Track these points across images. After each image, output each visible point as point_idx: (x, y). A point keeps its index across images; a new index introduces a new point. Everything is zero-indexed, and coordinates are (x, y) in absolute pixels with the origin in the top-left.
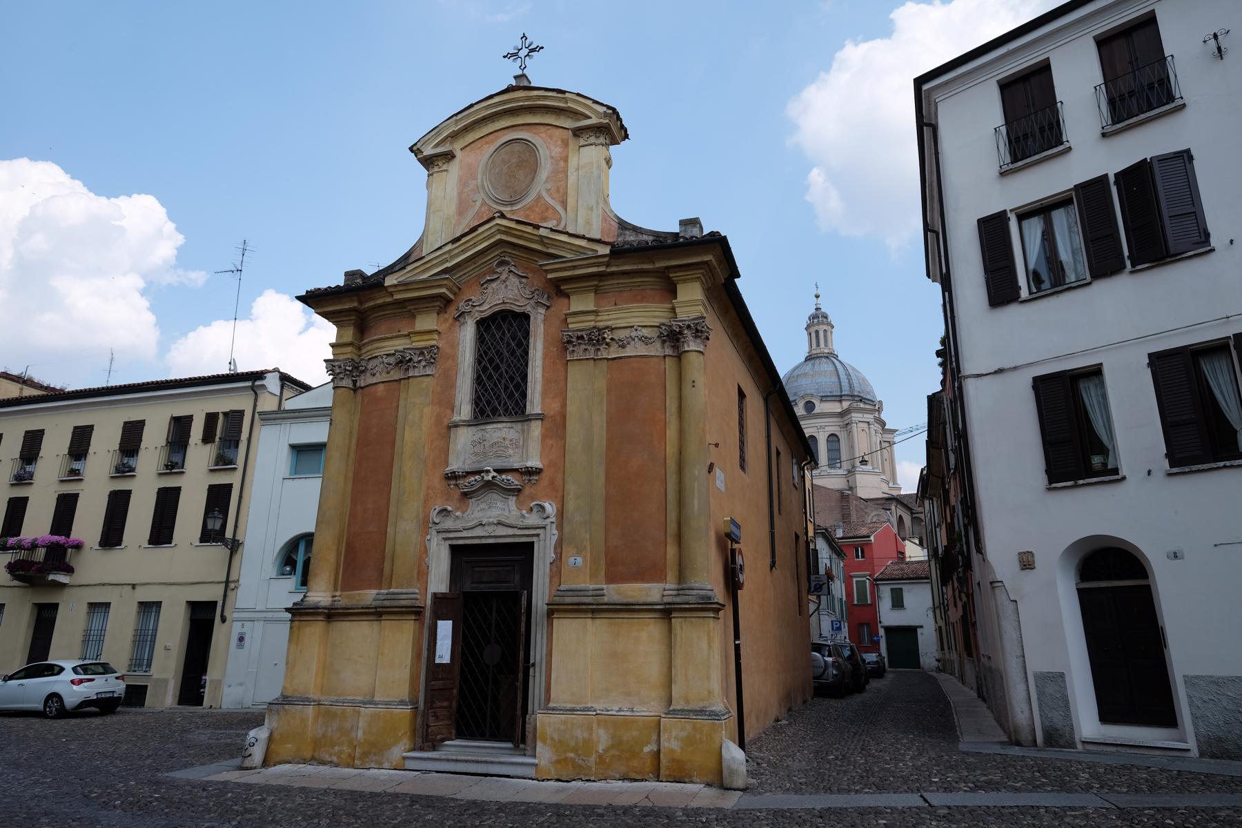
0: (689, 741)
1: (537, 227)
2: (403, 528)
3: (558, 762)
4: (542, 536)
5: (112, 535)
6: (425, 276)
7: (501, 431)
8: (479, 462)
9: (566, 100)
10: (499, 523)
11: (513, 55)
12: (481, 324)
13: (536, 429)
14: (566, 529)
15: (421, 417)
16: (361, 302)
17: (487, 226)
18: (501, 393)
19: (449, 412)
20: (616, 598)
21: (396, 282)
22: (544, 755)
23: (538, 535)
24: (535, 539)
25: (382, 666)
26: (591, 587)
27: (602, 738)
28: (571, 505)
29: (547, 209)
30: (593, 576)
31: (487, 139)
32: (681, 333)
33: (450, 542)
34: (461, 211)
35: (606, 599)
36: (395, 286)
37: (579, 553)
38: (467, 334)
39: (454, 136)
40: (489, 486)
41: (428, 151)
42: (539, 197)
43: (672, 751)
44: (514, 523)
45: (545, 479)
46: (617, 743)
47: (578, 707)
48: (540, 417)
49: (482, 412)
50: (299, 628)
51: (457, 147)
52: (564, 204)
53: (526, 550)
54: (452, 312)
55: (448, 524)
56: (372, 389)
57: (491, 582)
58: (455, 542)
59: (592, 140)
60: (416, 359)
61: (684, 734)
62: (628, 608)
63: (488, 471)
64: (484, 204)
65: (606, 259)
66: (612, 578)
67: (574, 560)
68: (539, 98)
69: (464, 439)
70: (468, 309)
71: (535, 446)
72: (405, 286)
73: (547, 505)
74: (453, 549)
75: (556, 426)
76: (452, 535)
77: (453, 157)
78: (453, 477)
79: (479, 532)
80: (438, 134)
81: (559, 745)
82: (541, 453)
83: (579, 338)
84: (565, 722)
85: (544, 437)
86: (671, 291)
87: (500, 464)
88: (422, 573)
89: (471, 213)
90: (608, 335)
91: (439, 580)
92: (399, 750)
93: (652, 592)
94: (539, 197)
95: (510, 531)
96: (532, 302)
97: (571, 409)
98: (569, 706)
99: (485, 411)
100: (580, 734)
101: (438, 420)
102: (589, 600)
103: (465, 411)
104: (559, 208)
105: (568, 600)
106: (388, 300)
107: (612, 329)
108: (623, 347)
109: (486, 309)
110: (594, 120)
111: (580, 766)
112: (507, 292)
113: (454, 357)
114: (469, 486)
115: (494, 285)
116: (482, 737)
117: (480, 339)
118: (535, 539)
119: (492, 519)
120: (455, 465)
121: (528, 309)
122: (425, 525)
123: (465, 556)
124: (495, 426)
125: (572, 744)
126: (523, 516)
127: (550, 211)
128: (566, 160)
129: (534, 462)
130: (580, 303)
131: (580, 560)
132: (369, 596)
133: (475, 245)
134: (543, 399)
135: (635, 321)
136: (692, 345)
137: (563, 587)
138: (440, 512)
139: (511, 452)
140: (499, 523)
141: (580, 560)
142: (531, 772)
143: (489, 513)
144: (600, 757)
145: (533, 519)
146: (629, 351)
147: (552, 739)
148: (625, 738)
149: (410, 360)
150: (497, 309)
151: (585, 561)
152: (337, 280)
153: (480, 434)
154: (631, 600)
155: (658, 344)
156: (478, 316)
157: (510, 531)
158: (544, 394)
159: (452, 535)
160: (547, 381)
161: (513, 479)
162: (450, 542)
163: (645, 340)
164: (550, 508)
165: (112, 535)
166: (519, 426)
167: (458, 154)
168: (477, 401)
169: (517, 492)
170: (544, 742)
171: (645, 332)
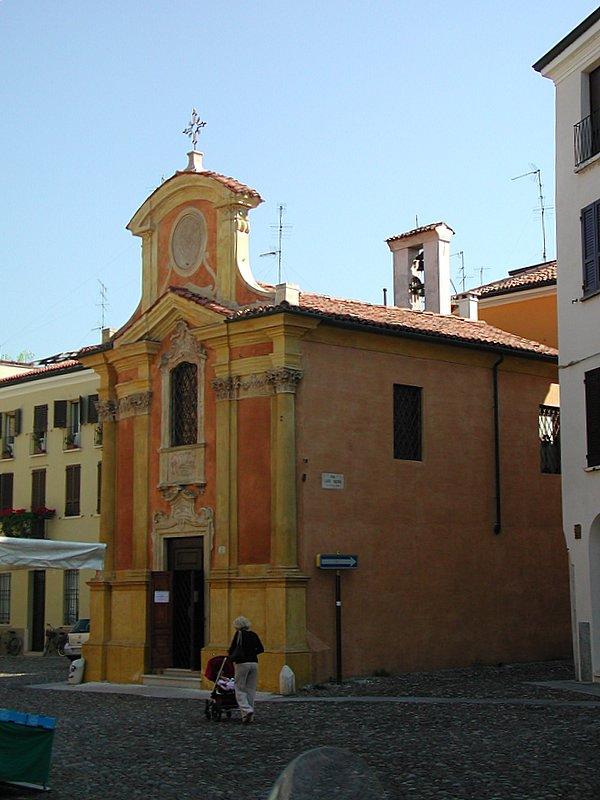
7: (182, 455)
14: (218, 527)
25: (130, 617)
28: (219, 510)
34: (160, 280)
42: (202, 267)
52: (215, 270)
70: (165, 362)
71: (200, 465)
78: (162, 490)
87: (183, 480)
89: (165, 285)
91: (159, 566)
104: (213, 274)
108: (246, 389)
109: (174, 362)
119: (183, 520)
120: (162, 481)
122: (149, 526)
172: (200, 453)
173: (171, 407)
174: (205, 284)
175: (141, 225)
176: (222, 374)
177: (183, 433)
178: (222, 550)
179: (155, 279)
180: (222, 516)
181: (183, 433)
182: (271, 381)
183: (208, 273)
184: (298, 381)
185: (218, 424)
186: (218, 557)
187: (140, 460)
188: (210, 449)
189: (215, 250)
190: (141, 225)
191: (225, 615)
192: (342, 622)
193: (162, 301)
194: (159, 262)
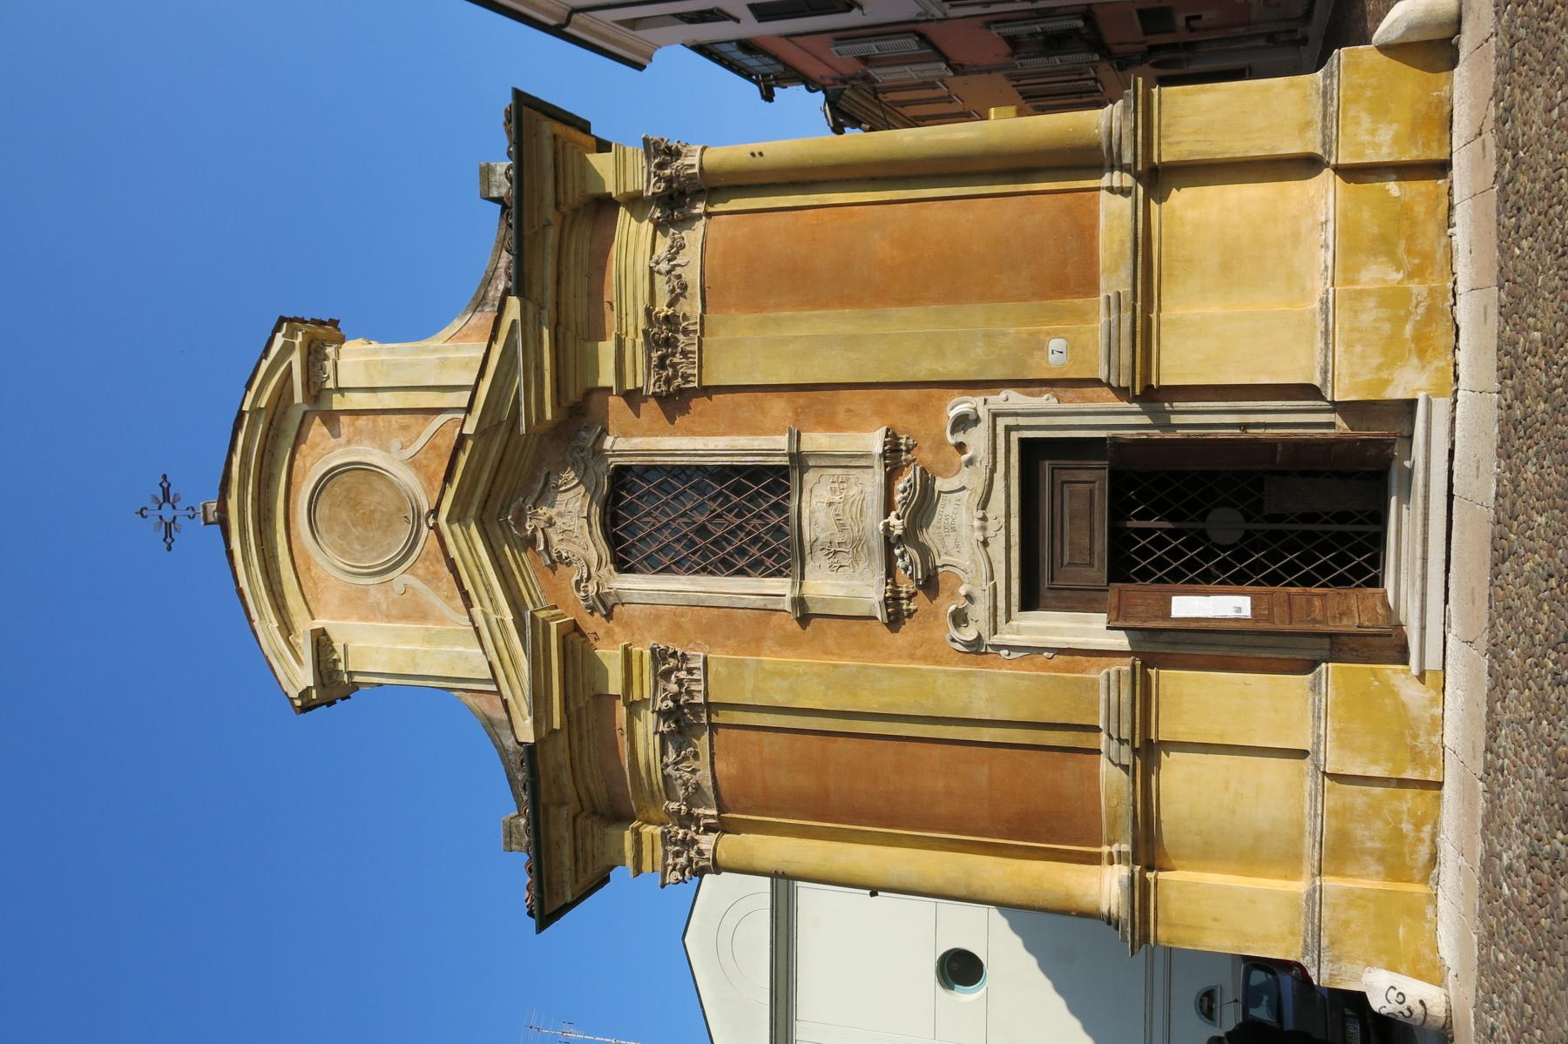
0: (1380, 110)
1: (462, 438)
3: (1421, 354)
4: (1011, 421)
6: (524, 664)
8: (870, 552)
9: (256, 411)
10: (984, 504)
11: (168, 533)
12: (622, 565)
15: (781, 674)
16: (562, 803)
17: (449, 540)
18: (746, 515)
19: (776, 619)
20: (1125, 274)
21: (529, 721)
23: (1008, 429)
24: (1015, 436)
26: (1103, 319)
27: (1377, 274)
29: (434, 447)
30: (1083, 316)
31: (301, 569)
32: (669, 180)
33: (1015, 608)
35: (1126, 289)
36: (536, 722)
37: (1042, 346)
38: (636, 585)
42: (414, 463)
43: (1396, 140)
45: (910, 427)
46: (1384, 247)
47: (1321, 327)
50: (1170, 925)
51: (304, 626)
53: (1033, 452)
54: (593, 624)
55: (979, 612)
56: (723, 784)
57: (1092, 529)
58: (1015, 599)
59: (329, 365)
60: (674, 688)
61: (1366, 121)
63: (887, 526)
65: (530, 306)
66: (1090, 286)
67: (1055, 357)
68: (244, 463)
69: (824, 584)
74: (1030, 602)
75: (815, 396)
76: (1001, 604)
77: (323, 632)
79: (997, 548)
81: (1392, 352)
84: (1349, 345)
85: (831, 425)
90: (662, 308)
91: (1090, 629)
96: (591, 463)
98: (1320, 344)
99: (781, 551)
100: (1370, 315)
101: (788, 642)
102: (1126, 316)
105: (1126, 358)
106: (562, 740)
110: (296, 359)
111: (1429, 309)
115: (555, 538)
116: (1379, 540)
117: (654, 565)
118: (1015, 436)
124: (805, 523)
125: (1387, 328)
126: (970, 462)
127: (439, 441)
129: (875, 442)
131: (1056, 344)
133: (480, 567)
134: (764, 433)
135: (643, 263)
138: (957, 625)
139: (854, 491)
140: (984, 504)
141: (1056, 344)
143: (964, 531)
144: (1410, 276)
145: (977, 440)
146: (692, 276)
147: (1379, 368)
148: (1375, 230)
149: (675, 698)
150: (597, 531)
151: (1056, 334)
153: (820, 554)
154: (1129, 245)
158: (755, 431)
159: (1001, 604)
162: (1015, 608)
163: (677, 249)
164: (962, 404)
167: (319, 623)
168: (755, 568)
170: (1386, 383)
190: (298, 660)
193: (454, 553)
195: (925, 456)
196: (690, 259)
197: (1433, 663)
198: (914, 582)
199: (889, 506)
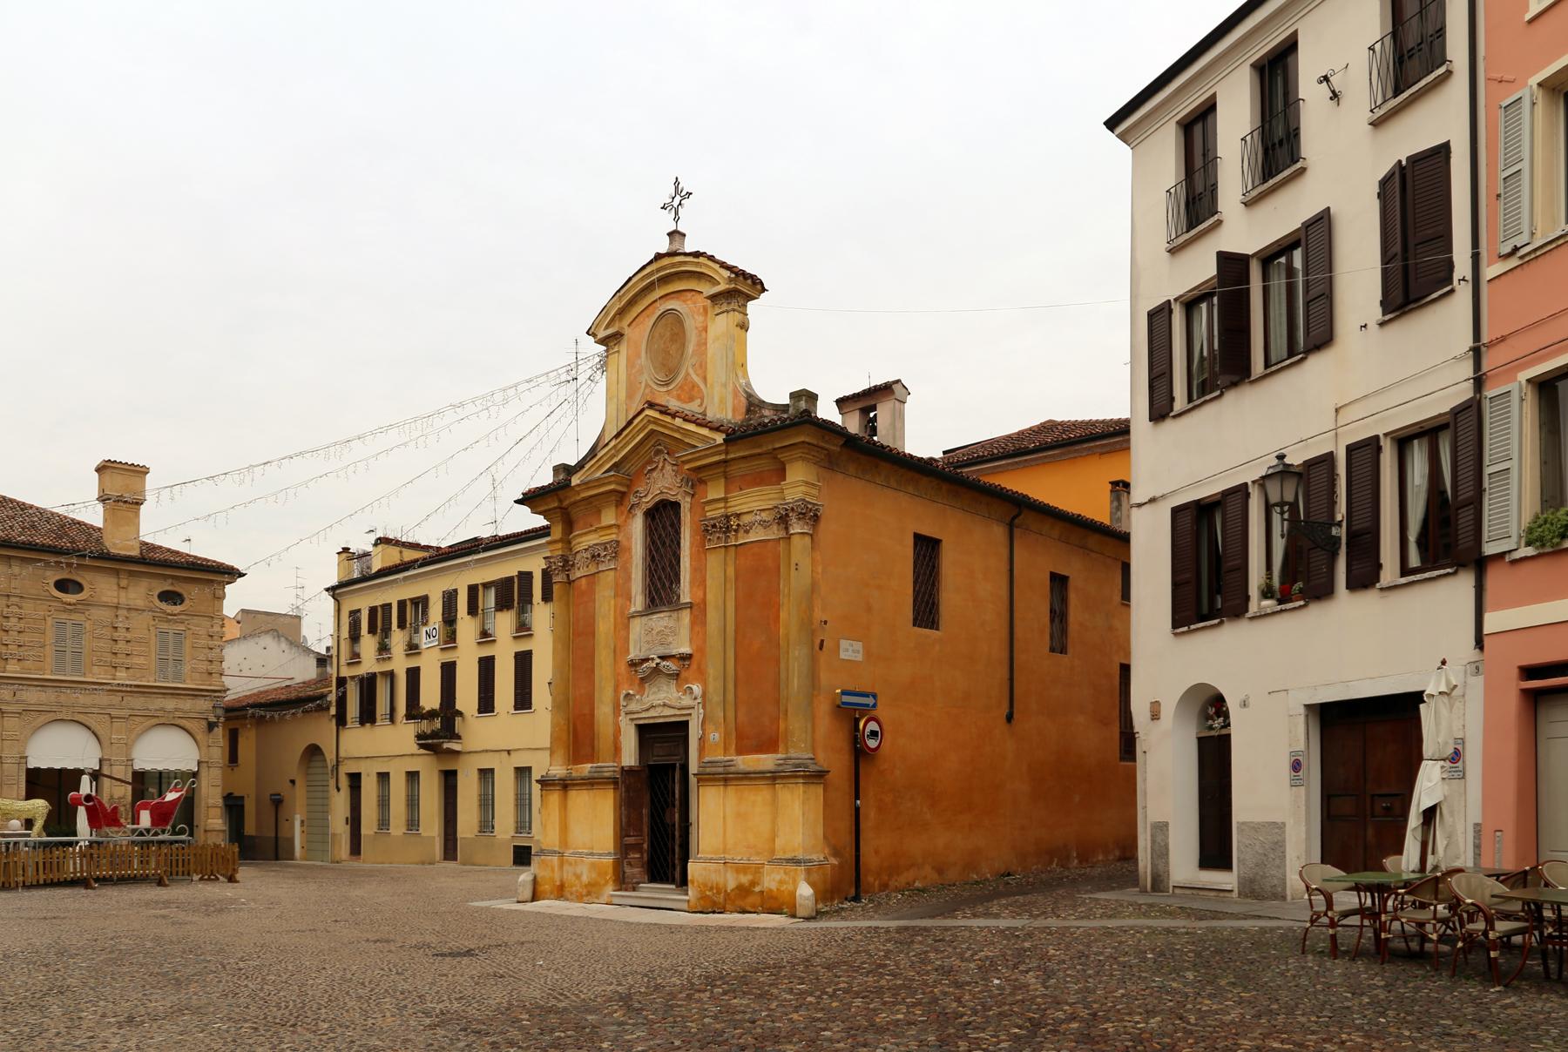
2: (603, 711)
5: (486, 704)
6: (598, 474)
7: (661, 621)
13: (686, 616)
22: (692, 892)
28: (711, 688)
34: (630, 396)
35: (732, 769)
37: (716, 730)
38: (637, 526)
39: (621, 312)
40: (656, 671)
41: (602, 334)
44: (673, 703)
48: (690, 606)
49: (652, 600)
52: (705, 379)
53: (684, 725)
55: (633, 706)
62: (747, 777)
64: (647, 385)
66: (740, 751)
69: (637, 626)
71: (685, 632)
72: (586, 485)
73: (694, 687)
78: (633, 664)
79: (652, 713)
80: (607, 314)
82: (691, 640)
83: (714, 526)
85: (693, 623)
86: (781, 474)
87: (663, 651)
88: (617, 750)
89: (638, 397)
91: (630, 756)
92: (609, 890)
93: (766, 761)
94: (688, 374)
95: (672, 712)
97: (710, 597)
103: (638, 602)
104: (702, 386)
107: (738, 516)
109: (648, 501)
112: (663, 483)
113: (630, 549)
114: (645, 672)
119: (662, 701)
120: (634, 654)
121: (679, 497)
122: (617, 709)
123: (647, 732)
128: (705, 329)
130: (715, 491)
132: (586, 769)
133: (633, 438)
135: (755, 506)
136: (796, 528)
137: (707, 759)
142: (685, 906)
146: (752, 537)
152: (546, 478)
155: (775, 527)
156: (645, 507)
157: (672, 712)
158: (692, 583)
160: (694, 570)
161: (671, 666)
163: (764, 524)
165: (486, 704)
166: (675, 615)
167: (627, 331)
169: (676, 676)
171: (764, 516)
172: (686, 616)
173: (645, 559)
174: (691, 399)
175: (607, 327)
176: (714, 512)
177: (662, 588)
178: (715, 736)
179: (623, 395)
180: (715, 697)
181: (662, 588)
182: (783, 520)
183: (694, 386)
184: (816, 518)
185: (704, 573)
186: (706, 744)
187: (604, 627)
188: (698, 610)
189: (704, 353)
190: (607, 327)
191: (719, 823)
192: (862, 826)
194: (629, 375)
195: (684, 674)
196: (756, 535)
197: (616, 901)
198: (645, 672)
199: (663, 658)
